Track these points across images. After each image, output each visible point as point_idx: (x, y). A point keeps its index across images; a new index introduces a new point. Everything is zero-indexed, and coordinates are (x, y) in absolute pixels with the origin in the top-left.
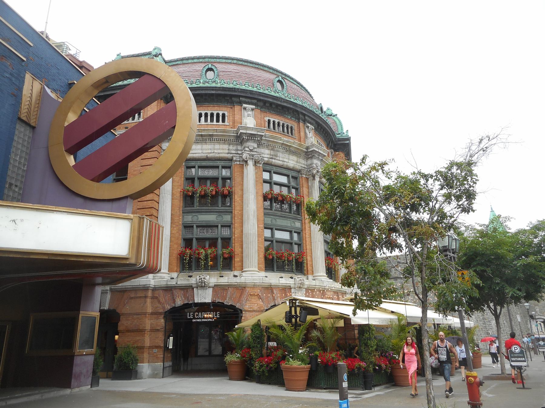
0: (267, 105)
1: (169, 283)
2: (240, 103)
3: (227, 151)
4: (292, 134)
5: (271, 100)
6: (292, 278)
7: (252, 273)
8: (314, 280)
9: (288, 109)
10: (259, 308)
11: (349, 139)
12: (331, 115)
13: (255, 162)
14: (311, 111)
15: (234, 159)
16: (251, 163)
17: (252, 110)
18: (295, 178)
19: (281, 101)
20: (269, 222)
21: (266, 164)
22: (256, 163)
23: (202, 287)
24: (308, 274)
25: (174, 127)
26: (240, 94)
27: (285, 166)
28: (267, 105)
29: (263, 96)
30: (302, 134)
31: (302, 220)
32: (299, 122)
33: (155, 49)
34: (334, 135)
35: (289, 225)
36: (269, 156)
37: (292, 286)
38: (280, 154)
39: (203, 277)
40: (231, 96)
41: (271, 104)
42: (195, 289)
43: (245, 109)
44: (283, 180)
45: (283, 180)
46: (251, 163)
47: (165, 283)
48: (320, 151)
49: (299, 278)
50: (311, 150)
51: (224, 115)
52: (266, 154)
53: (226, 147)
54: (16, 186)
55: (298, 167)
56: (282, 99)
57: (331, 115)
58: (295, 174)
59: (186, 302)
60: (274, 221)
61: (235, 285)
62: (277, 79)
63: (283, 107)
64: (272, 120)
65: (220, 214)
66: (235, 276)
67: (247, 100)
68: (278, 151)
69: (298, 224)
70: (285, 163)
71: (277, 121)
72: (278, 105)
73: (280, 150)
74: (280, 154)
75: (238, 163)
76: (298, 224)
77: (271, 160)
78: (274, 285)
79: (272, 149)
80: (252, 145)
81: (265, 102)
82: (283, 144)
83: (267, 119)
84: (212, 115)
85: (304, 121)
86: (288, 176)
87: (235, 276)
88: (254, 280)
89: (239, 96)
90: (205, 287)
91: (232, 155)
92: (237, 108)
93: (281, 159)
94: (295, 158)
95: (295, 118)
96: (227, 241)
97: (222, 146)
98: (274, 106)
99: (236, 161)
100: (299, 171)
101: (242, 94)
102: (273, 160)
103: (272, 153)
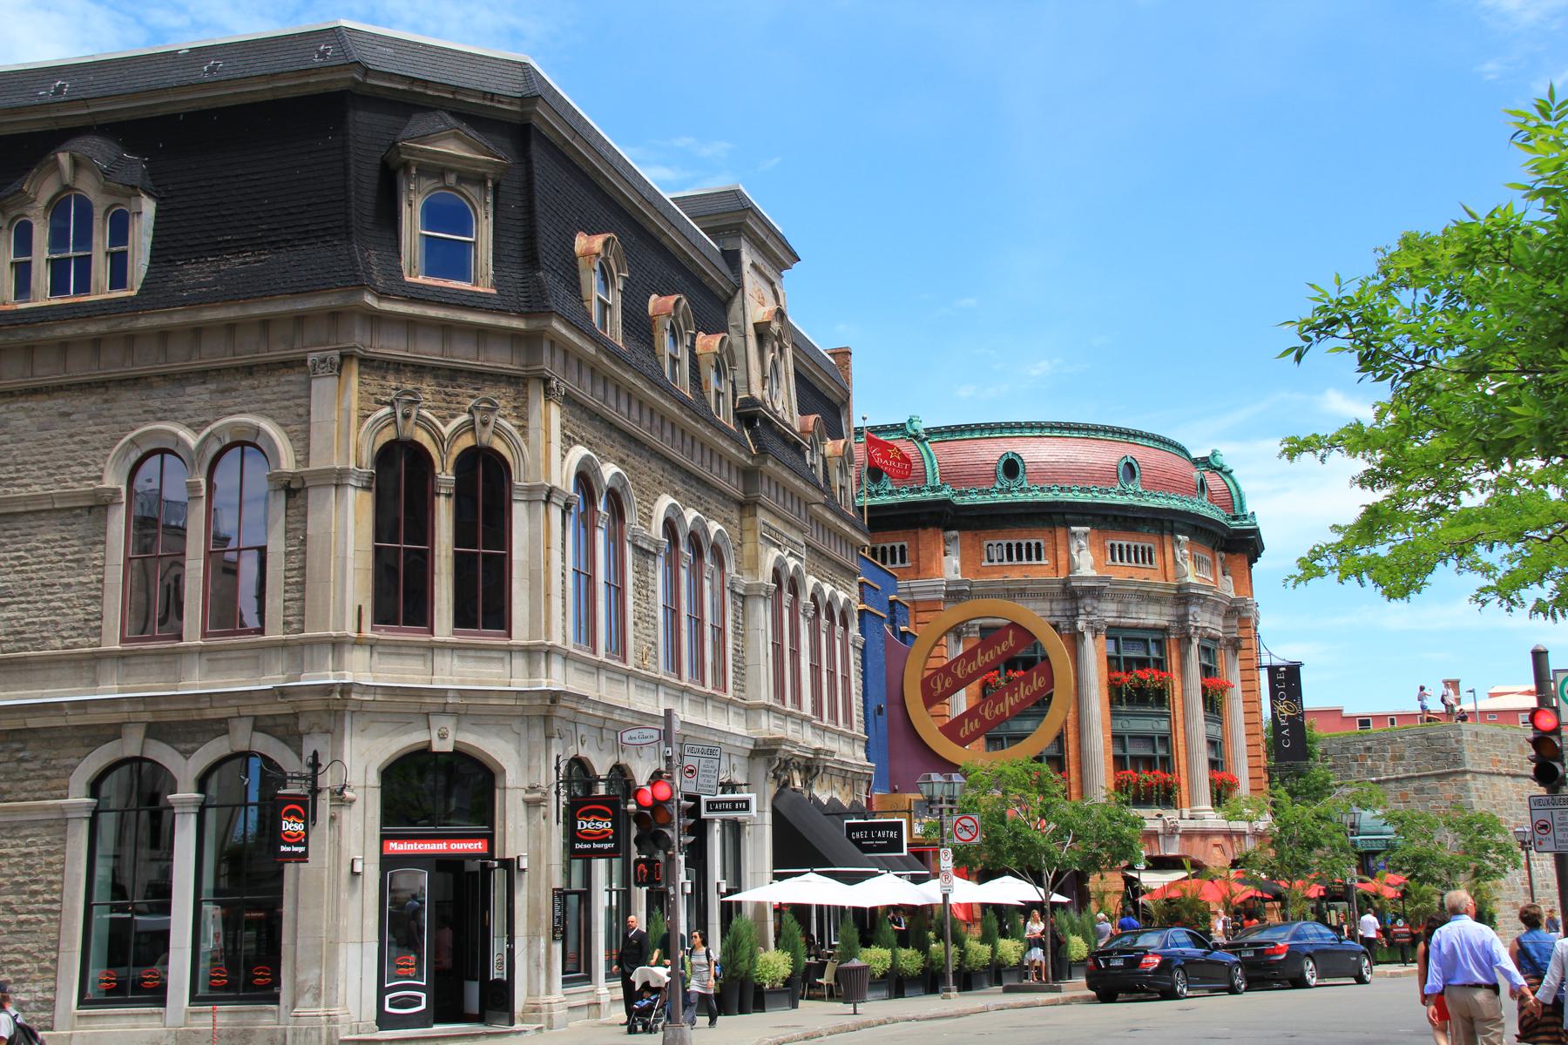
2: (1067, 524)
9: (1144, 520)
11: (1256, 532)
12: (1220, 469)
16: (1088, 636)
18: (1159, 644)
21: (1110, 627)
22: (1096, 632)
30: (1169, 557)
33: (911, 421)
37: (1160, 831)
38: (1133, 608)
40: (1049, 514)
41: (1115, 517)
46: (1088, 636)
49: (1170, 815)
51: (1038, 545)
52: (1109, 612)
53: (1047, 605)
57: (1220, 469)
58: (1158, 636)
64: (1117, 543)
69: (1164, 725)
71: (1125, 544)
72: (1125, 518)
76: (1164, 725)
81: (1105, 517)
84: (1019, 546)
89: (1063, 514)
92: (1060, 532)
94: (1155, 608)
97: (1040, 605)
103: (1121, 607)
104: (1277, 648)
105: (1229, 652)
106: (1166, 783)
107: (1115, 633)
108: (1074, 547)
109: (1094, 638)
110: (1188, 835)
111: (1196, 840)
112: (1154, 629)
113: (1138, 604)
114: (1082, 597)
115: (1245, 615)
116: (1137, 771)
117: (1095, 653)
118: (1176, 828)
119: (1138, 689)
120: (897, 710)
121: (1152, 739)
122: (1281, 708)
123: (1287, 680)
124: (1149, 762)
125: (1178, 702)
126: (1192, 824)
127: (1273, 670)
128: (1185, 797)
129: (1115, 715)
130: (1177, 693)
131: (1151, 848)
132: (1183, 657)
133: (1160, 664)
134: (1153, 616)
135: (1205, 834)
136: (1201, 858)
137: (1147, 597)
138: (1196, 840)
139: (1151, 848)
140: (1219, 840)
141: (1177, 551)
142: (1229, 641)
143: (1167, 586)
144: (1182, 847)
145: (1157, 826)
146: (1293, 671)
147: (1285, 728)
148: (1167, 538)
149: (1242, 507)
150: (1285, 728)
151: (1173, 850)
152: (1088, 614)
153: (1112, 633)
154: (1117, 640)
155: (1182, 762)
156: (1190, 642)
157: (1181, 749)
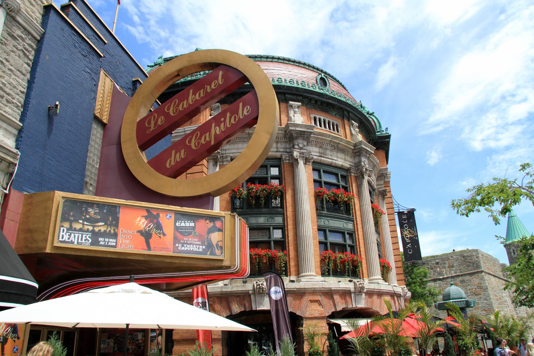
0: (313, 102)
1: (224, 290)
3: (275, 150)
4: (338, 132)
5: (316, 97)
6: (350, 281)
7: (313, 278)
8: (372, 283)
10: (320, 314)
13: (306, 160)
14: (355, 108)
15: (284, 157)
16: (301, 162)
17: (298, 107)
18: (344, 177)
19: (326, 98)
20: (322, 224)
23: (259, 293)
24: (363, 277)
25: (256, 118)
26: (285, 91)
27: (333, 165)
28: (313, 102)
29: (307, 93)
31: (353, 221)
32: (343, 119)
34: (375, 133)
35: (342, 226)
36: (318, 154)
37: (352, 290)
38: (328, 152)
39: (260, 283)
41: (316, 101)
42: (252, 296)
43: (291, 106)
44: (332, 180)
45: (332, 180)
46: (301, 162)
47: (219, 290)
48: (367, 149)
50: (359, 147)
52: (314, 152)
54: (91, 185)
55: (347, 165)
56: (327, 95)
58: (344, 173)
59: (243, 309)
60: (326, 222)
61: (294, 291)
62: (320, 76)
63: (328, 104)
64: (318, 117)
65: (271, 216)
66: (293, 281)
67: (293, 97)
68: (326, 149)
69: (350, 226)
70: (334, 161)
71: (322, 118)
72: (322, 103)
73: (328, 147)
74: (328, 152)
75: (287, 162)
76: (350, 226)
77: (320, 158)
78: (335, 290)
79: (320, 147)
80: (301, 142)
81: (310, 99)
82: (331, 141)
83: (312, 116)
85: (349, 119)
86: (336, 175)
87: (293, 281)
88: (313, 285)
90: (262, 293)
91: (280, 154)
93: (329, 157)
95: (340, 115)
96: (282, 244)
98: (319, 103)
99: (285, 160)
100: (348, 170)
101: (288, 92)
102: (322, 158)
103: (321, 150)
104: (402, 200)
105: (380, 198)
106: (353, 261)
107: (318, 167)
108: (291, 113)
109: (305, 164)
110: (370, 294)
111: (375, 297)
112: (341, 168)
113: (331, 150)
114: (297, 138)
115: (387, 180)
116: (335, 252)
117: (305, 175)
118: (363, 288)
119: (334, 203)
120: (113, 150)
121: (343, 233)
122: (406, 233)
123: (408, 219)
124: (342, 247)
125: (358, 213)
126: (372, 286)
127: (400, 214)
128: (365, 271)
129: (319, 215)
130: (357, 207)
131: (346, 302)
132: (359, 187)
133: (345, 188)
134: (342, 161)
135: (380, 294)
136: (378, 310)
137: (337, 147)
138: (375, 297)
139: (346, 302)
140: (388, 298)
141: (352, 129)
142: (380, 192)
143: (348, 142)
144: (367, 302)
145: (350, 286)
146: (411, 214)
147: (409, 243)
148: (346, 122)
149: (380, 127)
150: (409, 243)
151: (362, 303)
152: (301, 148)
153: (317, 167)
154: (319, 171)
155: (362, 249)
156: (363, 178)
157: (361, 241)
